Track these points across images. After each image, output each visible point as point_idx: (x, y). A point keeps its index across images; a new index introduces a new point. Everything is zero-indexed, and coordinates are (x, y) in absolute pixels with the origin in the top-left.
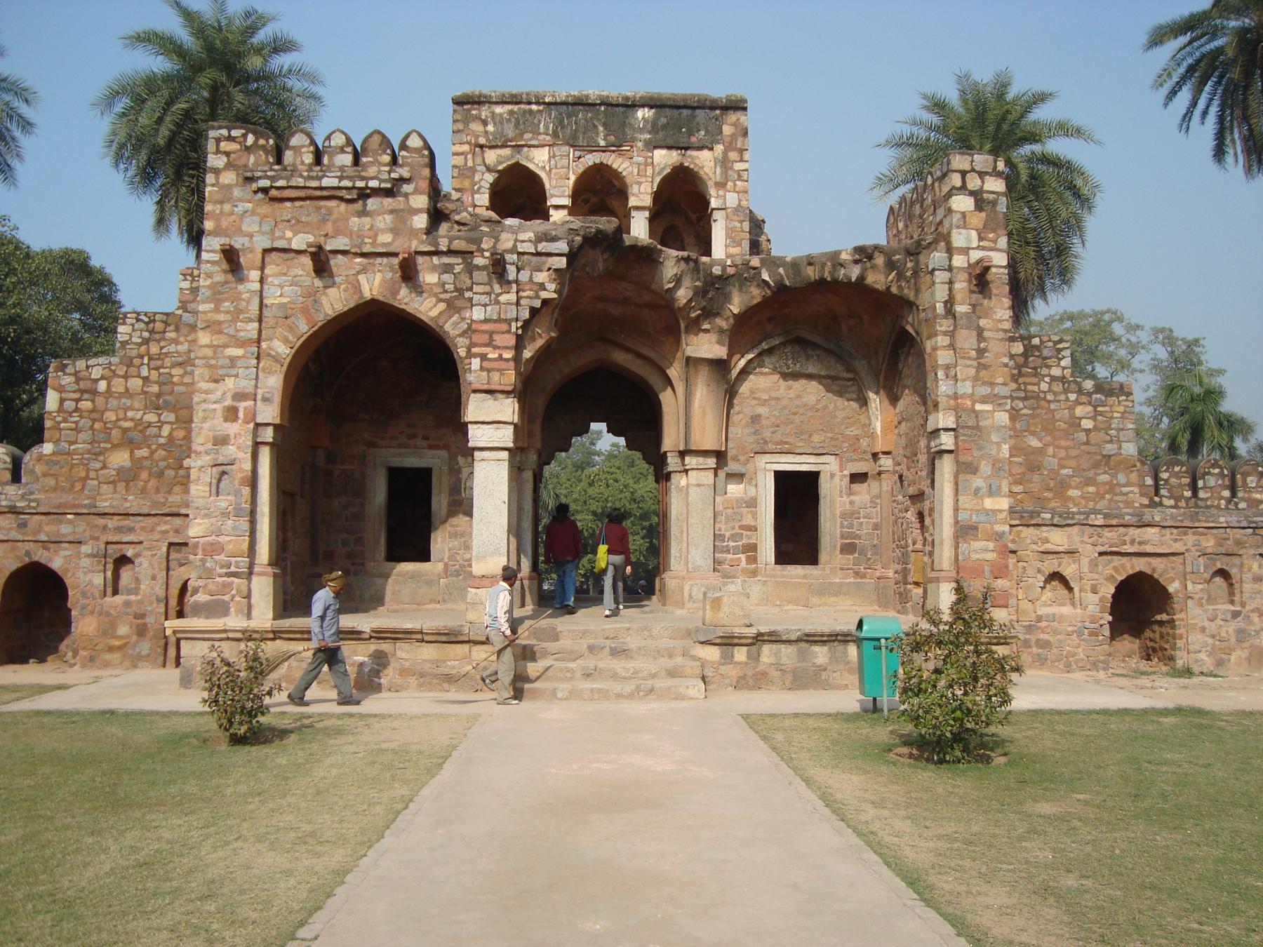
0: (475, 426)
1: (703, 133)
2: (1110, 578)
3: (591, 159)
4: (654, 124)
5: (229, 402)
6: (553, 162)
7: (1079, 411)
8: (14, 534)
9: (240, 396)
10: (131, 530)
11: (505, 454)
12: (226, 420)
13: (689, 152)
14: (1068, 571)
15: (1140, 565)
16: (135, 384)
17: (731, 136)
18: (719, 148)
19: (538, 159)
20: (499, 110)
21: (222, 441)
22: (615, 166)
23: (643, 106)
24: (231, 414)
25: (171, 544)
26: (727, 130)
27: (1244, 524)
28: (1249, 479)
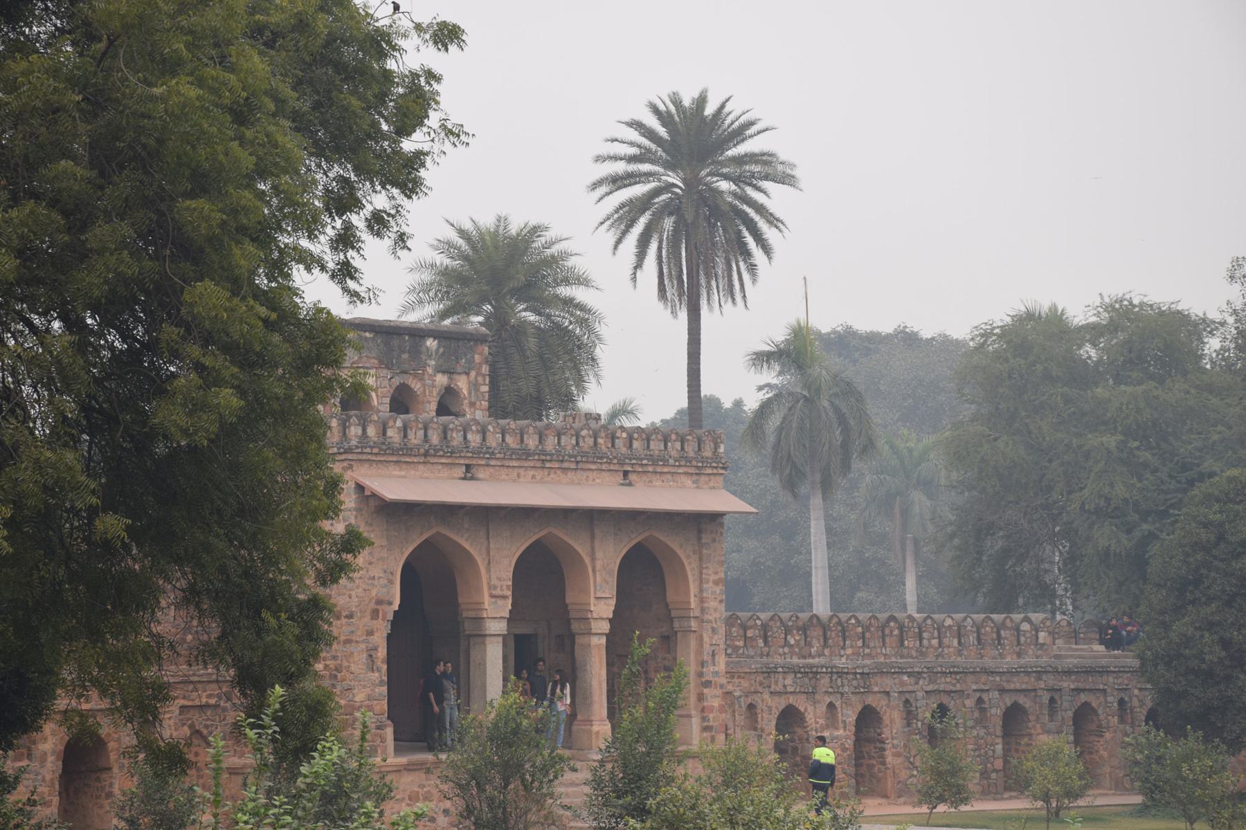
0: (490, 620)
1: (463, 361)
3: (397, 381)
5: (372, 605)
6: (378, 383)
9: (379, 602)
11: (500, 639)
12: (372, 619)
13: (455, 376)
17: (479, 363)
18: (473, 374)
21: (370, 633)
22: (412, 386)
23: (429, 337)
25: (182, 707)
27: (764, 670)
28: (734, 629)
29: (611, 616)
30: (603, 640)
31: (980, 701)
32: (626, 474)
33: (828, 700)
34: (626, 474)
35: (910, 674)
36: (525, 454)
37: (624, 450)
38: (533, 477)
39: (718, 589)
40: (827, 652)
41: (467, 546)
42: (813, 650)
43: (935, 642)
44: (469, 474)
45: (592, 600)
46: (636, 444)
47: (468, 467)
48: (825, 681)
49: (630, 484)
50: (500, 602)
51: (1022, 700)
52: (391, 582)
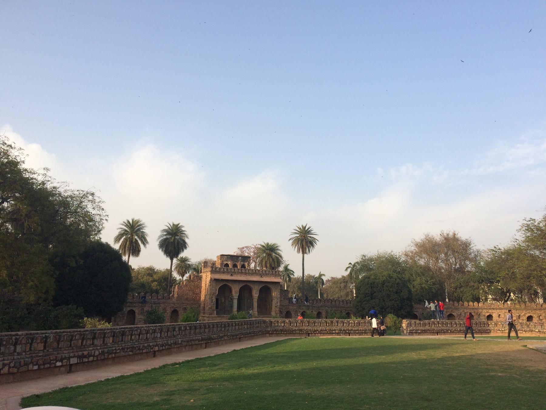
2: (285, 311)
3: (234, 263)
4: (241, 259)
5: (213, 293)
7: (283, 293)
8: (173, 306)
9: (214, 293)
10: (187, 306)
14: (281, 310)
15: (288, 310)
16: (187, 288)
19: (229, 263)
20: (225, 257)
24: (213, 295)
26: (249, 260)
29: (258, 296)
30: (257, 300)
31: (341, 311)
32: (261, 276)
33: (311, 310)
34: (261, 276)
35: (328, 307)
36: (242, 273)
37: (261, 273)
38: (244, 276)
39: (278, 293)
40: (317, 304)
41: (231, 286)
42: (315, 303)
43: (338, 303)
44: (231, 275)
45: (254, 294)
46: (263, 272)
47: (231, 275)
48: (311, 308)
49: (262, 277)
50: (237, 294)
51: (350, 312)
52: (216, 290)
